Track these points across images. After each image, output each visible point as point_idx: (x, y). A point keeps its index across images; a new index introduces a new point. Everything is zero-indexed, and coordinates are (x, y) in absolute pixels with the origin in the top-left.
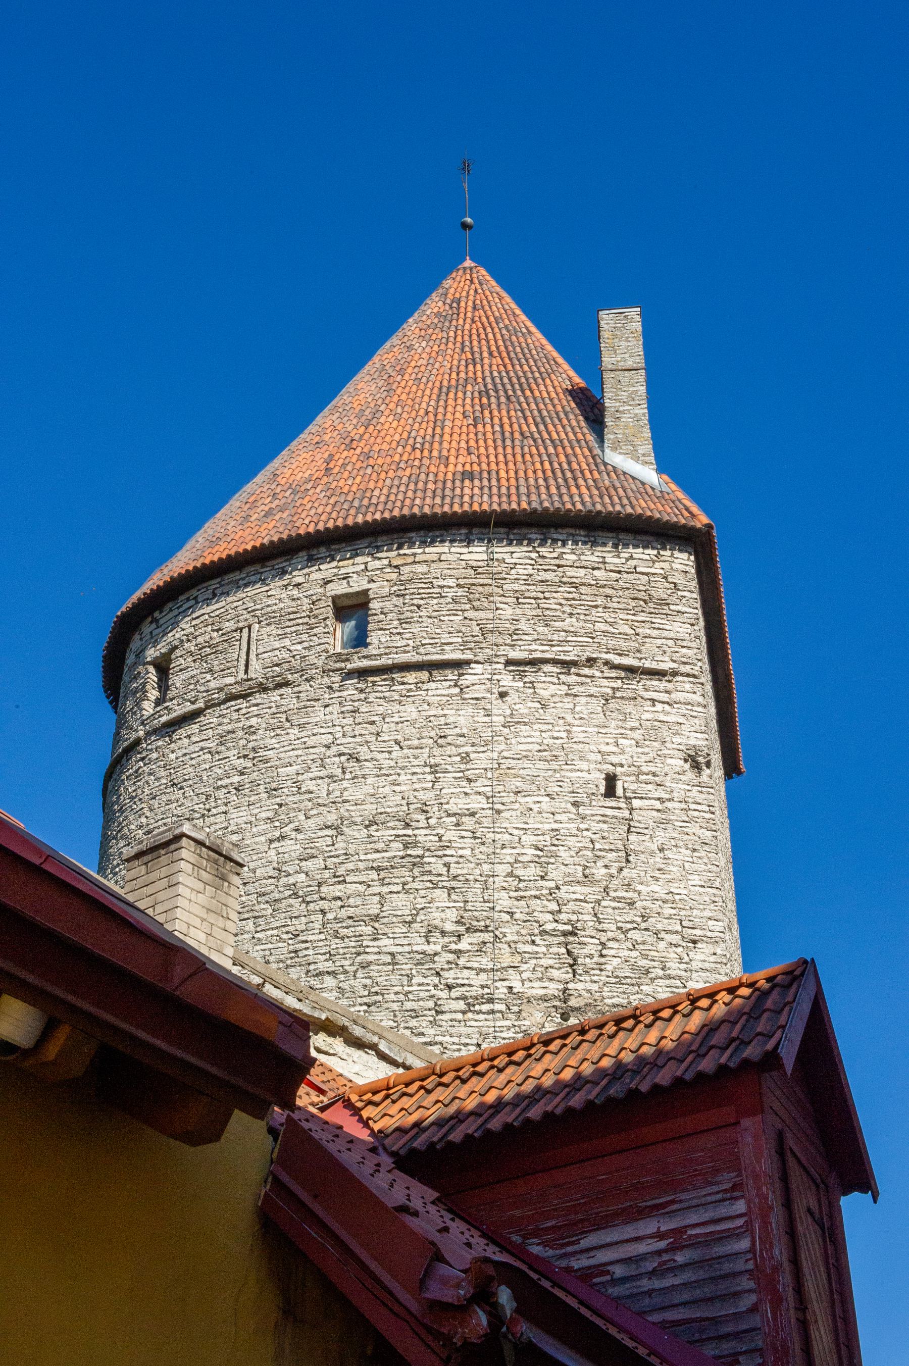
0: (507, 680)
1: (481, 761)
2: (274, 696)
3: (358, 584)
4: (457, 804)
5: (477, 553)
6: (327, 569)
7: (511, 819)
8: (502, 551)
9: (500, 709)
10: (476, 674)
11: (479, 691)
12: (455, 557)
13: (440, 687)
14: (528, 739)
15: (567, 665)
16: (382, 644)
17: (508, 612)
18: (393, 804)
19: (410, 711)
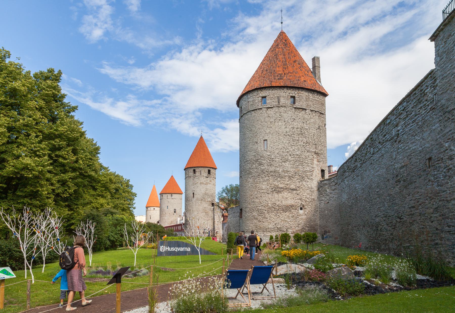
0: (310, 113)
1: (308, 122)
2: (284, 108)
3: (294, 95)
4: (306, 128)
5: (307, 94)
6: (290, 91)
7: (311, 130)
8: (309, 94)
9: (310, 116)
10: (307, 111)
11: (307, 113)
12: (304, 94)
13: (303, 112)
14: (312, 120)
15: (316, 111)
16: (297, 105)
17: (310, 103)
18: (299, 126)
19: (300, 114)
